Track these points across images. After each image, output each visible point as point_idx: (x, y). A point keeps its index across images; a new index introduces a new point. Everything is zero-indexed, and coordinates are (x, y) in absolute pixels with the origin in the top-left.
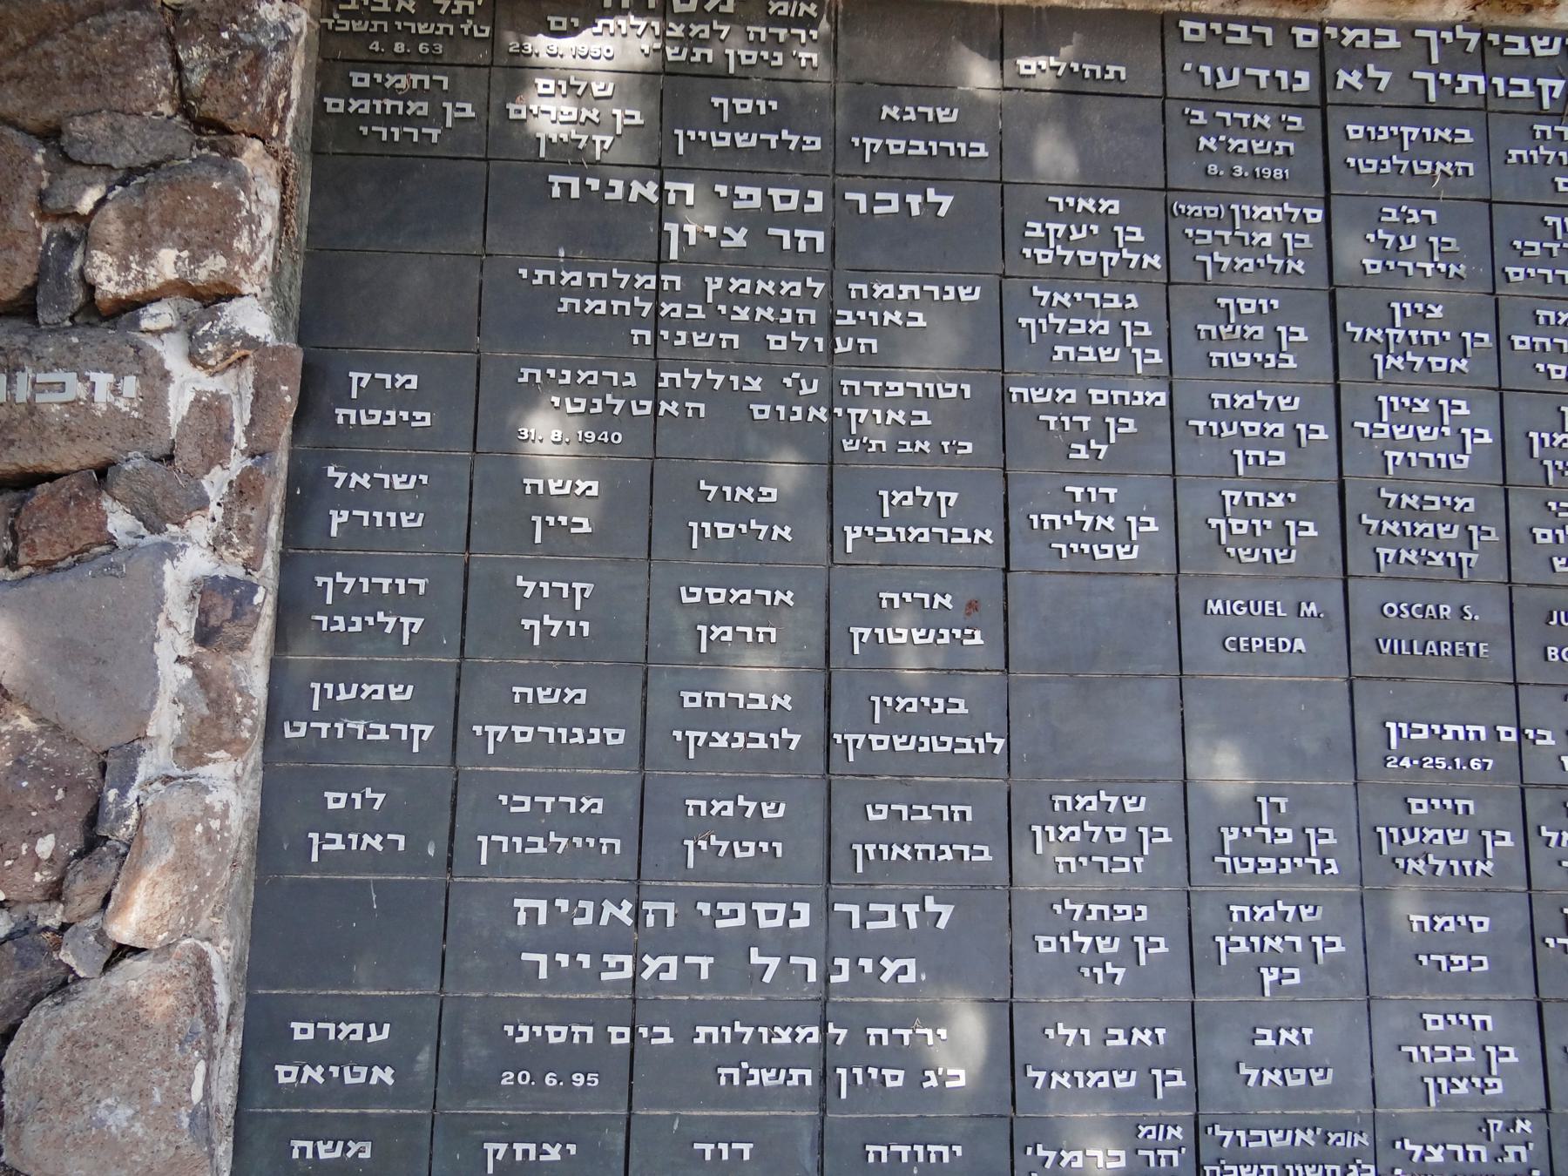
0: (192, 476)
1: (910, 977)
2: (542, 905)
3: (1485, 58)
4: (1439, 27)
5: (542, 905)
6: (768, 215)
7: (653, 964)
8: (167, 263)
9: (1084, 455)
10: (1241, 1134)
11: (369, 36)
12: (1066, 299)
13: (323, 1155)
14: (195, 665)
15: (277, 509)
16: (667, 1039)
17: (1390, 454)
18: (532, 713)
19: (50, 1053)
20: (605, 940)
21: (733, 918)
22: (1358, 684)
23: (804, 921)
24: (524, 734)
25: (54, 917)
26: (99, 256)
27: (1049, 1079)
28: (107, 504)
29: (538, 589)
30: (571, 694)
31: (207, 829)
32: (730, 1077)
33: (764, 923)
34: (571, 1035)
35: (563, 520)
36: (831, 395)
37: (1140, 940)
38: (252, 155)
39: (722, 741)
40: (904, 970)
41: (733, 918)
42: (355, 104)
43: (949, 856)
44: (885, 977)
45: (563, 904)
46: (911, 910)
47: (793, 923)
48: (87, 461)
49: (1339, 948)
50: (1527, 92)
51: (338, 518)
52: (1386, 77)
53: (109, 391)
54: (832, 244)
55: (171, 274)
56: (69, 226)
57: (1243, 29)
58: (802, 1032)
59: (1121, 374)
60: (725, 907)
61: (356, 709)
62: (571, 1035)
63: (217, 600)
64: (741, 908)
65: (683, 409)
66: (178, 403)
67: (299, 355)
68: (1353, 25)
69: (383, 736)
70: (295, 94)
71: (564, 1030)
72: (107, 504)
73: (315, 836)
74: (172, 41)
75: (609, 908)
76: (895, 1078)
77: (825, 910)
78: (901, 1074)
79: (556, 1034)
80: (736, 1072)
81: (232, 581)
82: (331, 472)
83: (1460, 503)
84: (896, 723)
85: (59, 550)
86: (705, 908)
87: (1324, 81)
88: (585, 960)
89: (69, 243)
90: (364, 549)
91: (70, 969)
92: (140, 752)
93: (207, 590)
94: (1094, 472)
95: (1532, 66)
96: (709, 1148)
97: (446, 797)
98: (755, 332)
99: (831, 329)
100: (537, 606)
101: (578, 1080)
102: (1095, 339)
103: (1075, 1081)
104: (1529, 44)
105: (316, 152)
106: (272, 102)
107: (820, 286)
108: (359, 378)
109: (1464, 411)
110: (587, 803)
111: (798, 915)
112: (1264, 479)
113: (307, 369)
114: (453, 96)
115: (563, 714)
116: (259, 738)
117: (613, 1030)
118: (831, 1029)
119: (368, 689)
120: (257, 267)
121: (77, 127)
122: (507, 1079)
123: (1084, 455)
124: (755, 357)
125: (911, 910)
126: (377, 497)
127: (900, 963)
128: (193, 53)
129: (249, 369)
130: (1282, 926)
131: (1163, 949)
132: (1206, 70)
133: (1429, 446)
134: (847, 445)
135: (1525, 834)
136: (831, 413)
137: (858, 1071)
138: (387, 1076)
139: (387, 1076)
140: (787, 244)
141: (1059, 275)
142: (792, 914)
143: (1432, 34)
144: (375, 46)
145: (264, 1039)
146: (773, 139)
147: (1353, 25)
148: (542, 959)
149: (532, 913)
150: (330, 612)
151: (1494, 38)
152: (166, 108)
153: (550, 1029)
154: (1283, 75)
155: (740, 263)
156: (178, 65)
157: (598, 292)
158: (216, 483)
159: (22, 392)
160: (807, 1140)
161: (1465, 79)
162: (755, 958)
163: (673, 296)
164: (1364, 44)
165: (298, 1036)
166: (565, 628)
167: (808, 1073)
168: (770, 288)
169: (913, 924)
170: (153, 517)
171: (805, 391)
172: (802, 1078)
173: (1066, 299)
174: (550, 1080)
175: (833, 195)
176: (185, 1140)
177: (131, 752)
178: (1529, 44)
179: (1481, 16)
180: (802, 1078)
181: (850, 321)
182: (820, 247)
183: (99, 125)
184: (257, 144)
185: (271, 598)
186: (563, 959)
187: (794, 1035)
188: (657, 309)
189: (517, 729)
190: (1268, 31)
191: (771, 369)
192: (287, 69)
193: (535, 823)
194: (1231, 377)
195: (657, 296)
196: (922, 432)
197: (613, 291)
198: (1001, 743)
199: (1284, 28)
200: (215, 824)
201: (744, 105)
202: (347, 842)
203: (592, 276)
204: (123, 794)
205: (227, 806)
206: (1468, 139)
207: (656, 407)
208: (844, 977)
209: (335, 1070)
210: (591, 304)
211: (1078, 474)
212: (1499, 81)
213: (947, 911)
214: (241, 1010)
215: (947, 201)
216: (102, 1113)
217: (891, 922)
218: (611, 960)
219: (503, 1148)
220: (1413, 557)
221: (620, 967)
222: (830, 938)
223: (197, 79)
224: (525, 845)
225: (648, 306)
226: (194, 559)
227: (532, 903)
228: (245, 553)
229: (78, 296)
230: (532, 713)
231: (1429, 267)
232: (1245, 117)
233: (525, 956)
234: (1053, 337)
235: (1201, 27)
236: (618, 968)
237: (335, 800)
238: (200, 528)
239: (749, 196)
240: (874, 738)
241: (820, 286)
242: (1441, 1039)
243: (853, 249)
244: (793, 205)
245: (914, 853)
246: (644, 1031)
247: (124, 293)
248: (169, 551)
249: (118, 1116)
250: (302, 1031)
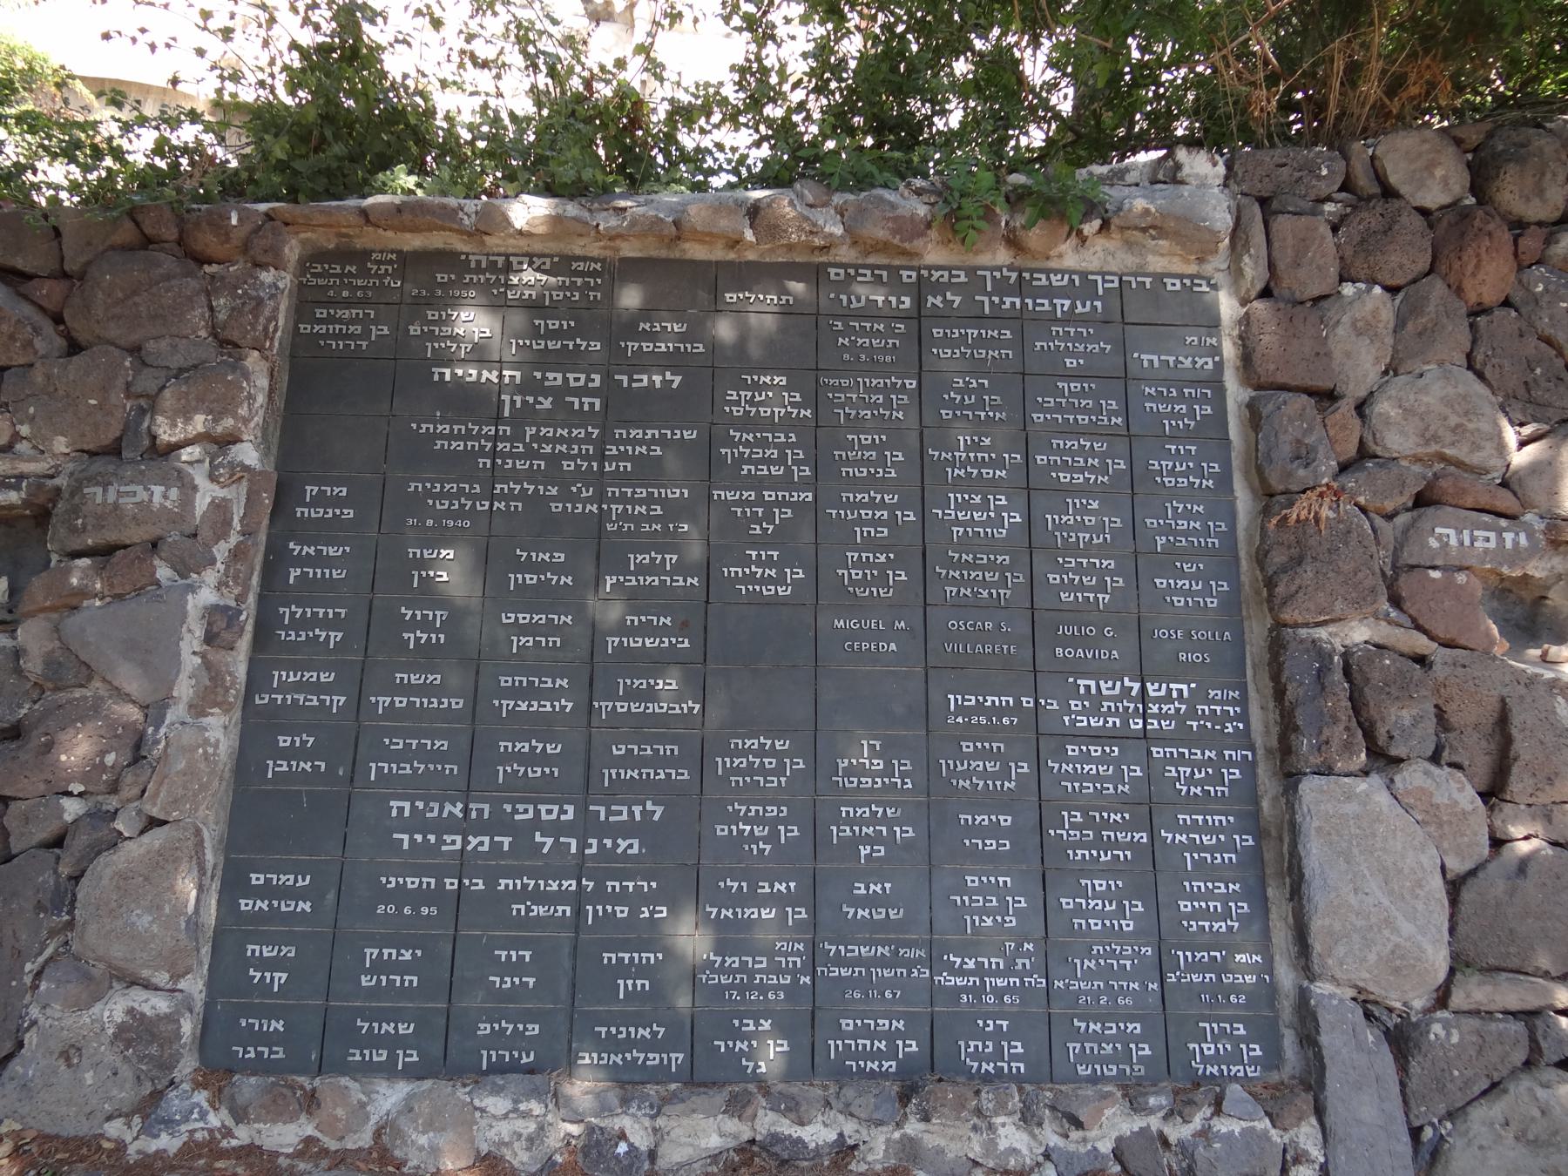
0: (208, 547)
1: (635, 850)
2: (407, 805)
3: (1021, 288)
4: (992, 269)
5: (407, 805)
6: (566, 389)
7: (474, 841)
8: (199, 423)
9: (758, 531)
10: (842, 948)
11: (328, 287)
12: (750, 437)
13: (265, 954)
14: (203, 656)
15: (258, 568)
16: (481, 887)
17: (955, 529)
18: (407, 689)
19: (105, 882)
20: (444, 826)
21: (525, 814)
22: (931, 672)
23: (570, 816)
24: (401, 702)
25: (112, 803)
26: (160, 419)
27: (719, 913)
28: (157, 562)
29: (414, 615)
30: (431, 678)
31: (205, 752)
32: (519, 910)
33: (544, 816)
34: (421, 883)
35: (431, 573)
36: (600, 497)
37: (782, 828)
38: (253, 360)
39: (524, 706)
40: (631, 846)
41: (525, 814)
42: (317, 328)
43: (662, 776)
44: (619, 851)
45: (420, 805)
46: (637, 809)
47: (563, 817)
48: (146, 537)
49: (911, 834)
50: (1047, 308)
51: (295, 573)
52: (958, 300)
53: (160, 496)
54: (605, 406)
55: (200, 428)
56: (143, 402)
57: (869, 273)
58: (565, 884)
59: (787, 482)
60: (521, 807)
61: (300, 687)
62: (421, 883)
63: (218, 617)
64: (531, 808)
65: (508, 507)
66: (201, 503)
67: (275, 476)
68: (938, 268)
69: (315, 703)
70: (281, 322)
71: (417, 881)
72: (157, 562)
73: (270, 763)
74: (208, 294)
75: (448, 807)
76: (622, 912)
77: (582, 811)
78: (626, 909)
79: (412, 883)
80: (523, 907)
81: (228, 608)
82: (291, 545)
83: (1000, 558)
84: (632, 695)
85: (128, 588)
86: (508, 808)
87: (919, 302)
88: (432, 838)
89: (142, 412)
90: (310, 591)
91: (120, 833)
92: (167, 706)
93: (212, 612)
94: (762, 543)
95: (1050, 292)
96: (504, 954)
97: (351, 739)
98: (554, 460)
99: (602, 457)
100: (413, 625)
101: (425, 911)
102: (769, 462)
103: (735, 914)
104: (1048, 278)
105: (292, 356)
106: (266, 329)
107: (596, 432)
108: (311, 490)
109: (1004, 502)
110: (438, 744)
111: (566, 812)
112: (872, 545)
113: (280, 485)
114: (376, 322)
115: (425, 690)
116: (240, 704)
117: (448, 881)
118: (584, 882)
119: (307, 675)
120: (252, 425)
121: (151, 346)
122: (381, 909)
123: (758, 531)
124: (552, 472)
125: (637, 809)
126: (319, 560)
127: (628, 842)
128: (221, 302)
129: (245, 483)
130: (874, 820)
131: (796, 833)
132: (844, 297)
133: (980, 524)
134: (609, 527)
135: (1038, 765)
136: (600, 508)
137: (600, 908)
138: (307, 907)
139: (307, 907)
140: (577, 407)
141: (747, 423)
142: (562, 812)
143: (988, 273)
144: (331, 293)
145: (233, 884)
146: (571, 344)
147: (938, 268)
148: (406, 837)
149: (400, 809)
150: (287, 628)
151: (1027, 275)
152: (203, 333)
153: (409, 880)
154: (893, 299)
155: (549, 418)
156: (211, 309)
157: (459, 437)
158: (221, 551)
159: (111, 497)
160: (566, 950)
161: (1008, 300)
162: (538, 838)
163: (505, 439)
164: (946, 279)
165: (254, 882)
166: (429, 638)
167: (568, 909)
168: (565, 433)
169: (638, 818)
170: (183, 569)
171: (584, 494)
172: (564, 912)
173: (750, 437)
174: (407, 910)
175: (607, 377)
176: (183, 936)
178: (1048, 278)
179: (1019, 262)
180: (564, 912)
181: (615, 452)
182: (597, 408)
183: (164, 344)
184: (256, 353)
185: (251, 621)
186: (419, 838)
187: (560, 885)
188: (495, 446)
189: (397, 699)
190: (885, 273)
191: (564, 481)
192: (276, 309)
193: (405, 755)
194: (855, 484)
195: (496, 438)
196: (657, 519)
197: (469, 436)
198: (697, 706)
199: (894, 271)
200: (210, 750)
201: (554, 324)
202: (290, 766)
203: (456, 428)
204: (157, 730)
205: (218, 741)
206: (1009, 336)
207: (492, 505)
208: (594, 850)
209: (275, 903)
210: (454, 444)
211: (756, 543)
212: (1029, 301)
213: (659, 810)
214: (221, 867)
215: (678, 379)
216: (134, 918)
217: (625, 817)
218: (448, 838)
219: (376, 952)
220: (968, 592)
221: (454, 843)
222: (586, 826)
223: (222, 316)
224: (399, 768)
225: (490, 445)
226: (207, 596)
227: (401, 804)
228: (237, 591)
229: (146, 442)
230: (407, 689)
231: (983, 414)
232: (868, 325)
233: (395, 836)
234: (741, 460)
235: (842, 271)
236: (453, 842)
237: (284, 741)
238: (211, 576)
239: (555, 378)
240: (618, 704)
241: (596, 432)
242: (977, 891)
243: (622, 407)
244: (582, 383)
245: (640, 774)
246: (466, 882)
247: (173, 439)
248: (192, 589)
249: (143, 921)
250: (257, 879)
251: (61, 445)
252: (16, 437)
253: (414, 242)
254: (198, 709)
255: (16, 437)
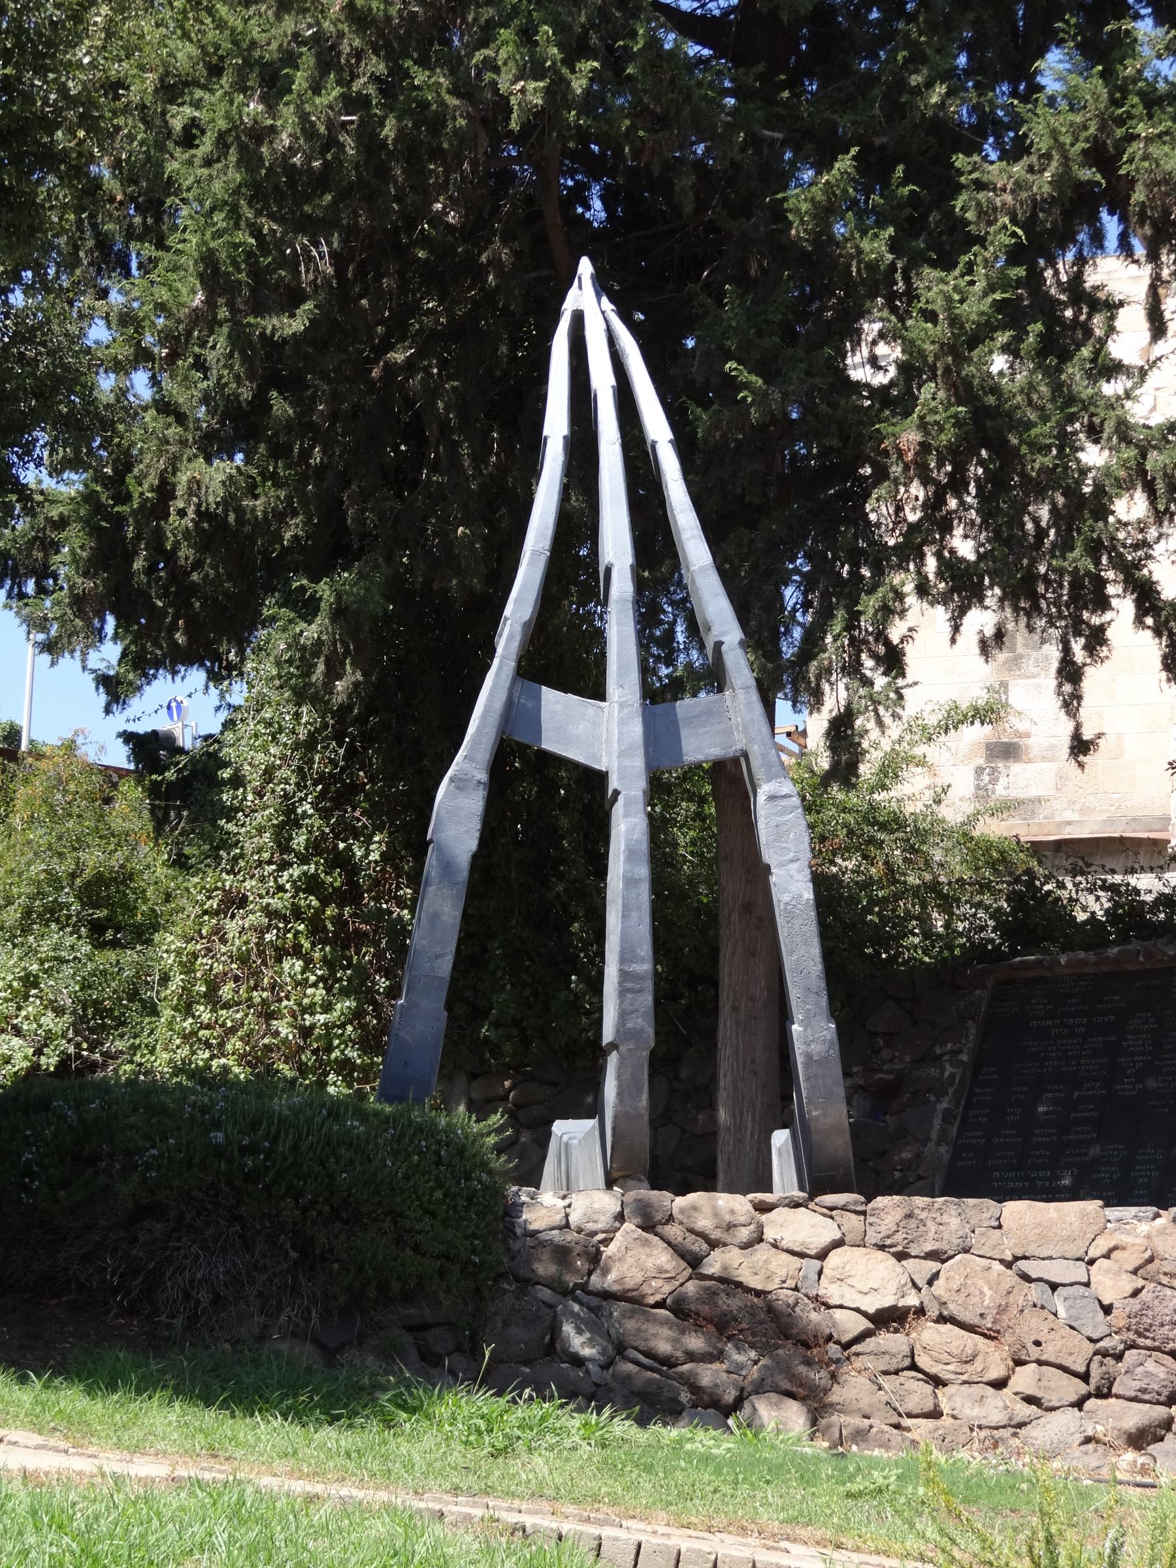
53: (933, 1072)
66: (947, 1074)
177: (928, 1139)
226: (945, 1105)
238: (947, 1099)
251: (907, 1059)
252: (894, 1057)
253: (1031, 974)
254: (938, 1144)
255: (894, 1057)
